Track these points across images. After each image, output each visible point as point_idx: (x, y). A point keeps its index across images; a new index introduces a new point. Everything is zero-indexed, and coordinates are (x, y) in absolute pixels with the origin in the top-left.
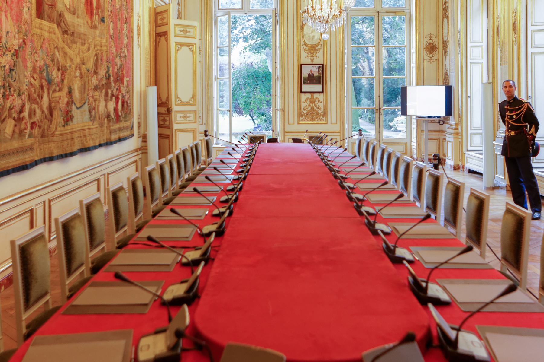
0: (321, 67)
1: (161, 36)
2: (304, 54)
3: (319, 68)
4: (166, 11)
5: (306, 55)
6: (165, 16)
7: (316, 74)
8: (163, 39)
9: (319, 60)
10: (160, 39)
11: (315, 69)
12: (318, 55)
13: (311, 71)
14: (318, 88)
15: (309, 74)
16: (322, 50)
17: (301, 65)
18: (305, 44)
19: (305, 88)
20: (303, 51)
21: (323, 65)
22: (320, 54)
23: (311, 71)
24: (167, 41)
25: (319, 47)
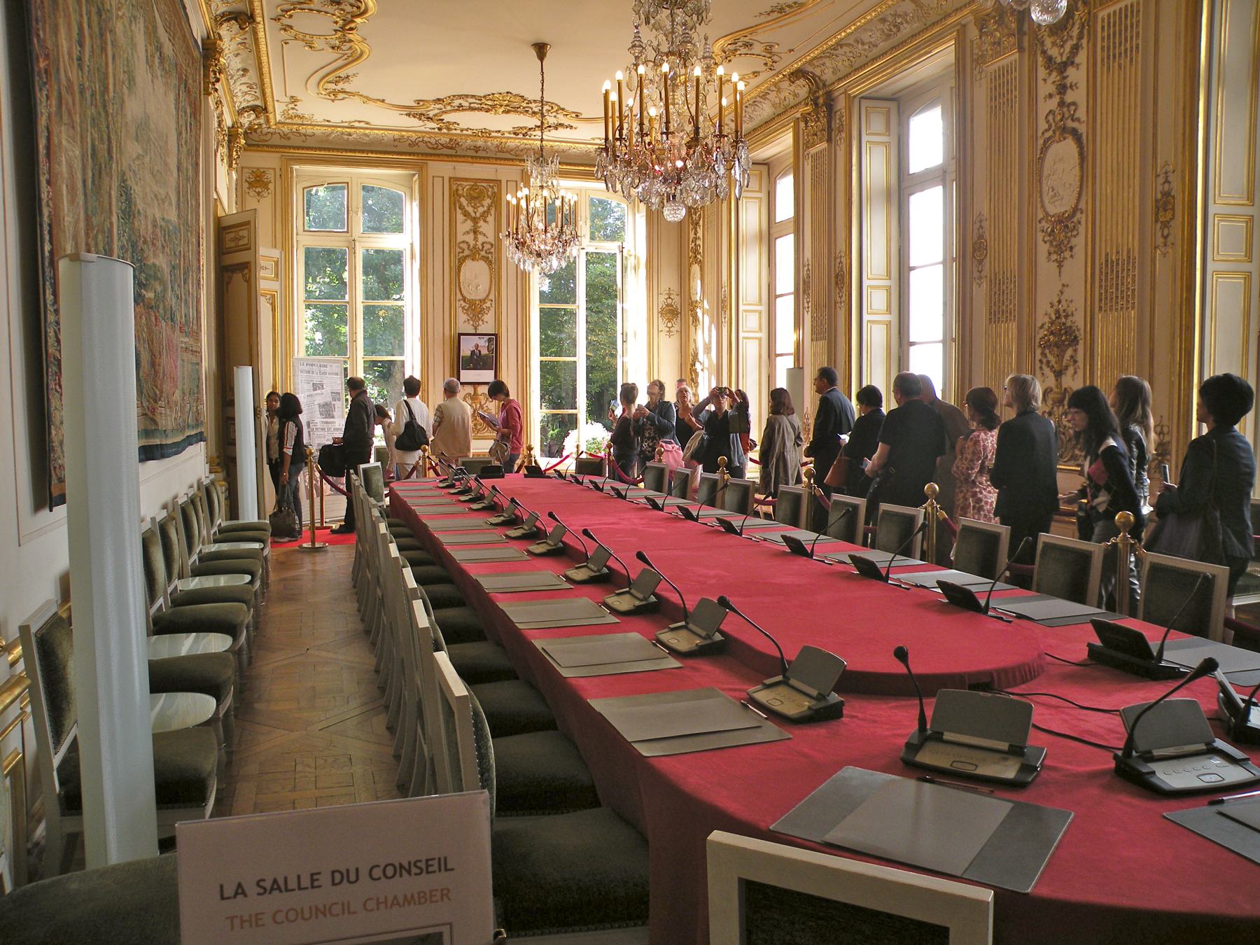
0: (494, 339)
1: (233, 272)
2: (462, 317)
3: (489, 340)
4: (248, 223)
5: (465, 317)
6: (244, 233)
7: (484, 352)
8: (238, 277)
9: (487, 326)
10: (230, 278)
11: (483, 343)
12: (486, 318)
13: (477, 346)
14: (488, 376)
15: (473, 352)
16: (492, 309)
17: (460, 335)
18: (464, 299)
19: (467, 375)
20: (460, 310)
21: (496, 335)
22: (489, 317)
23: (477, 346)
24: (248, 281)
25: (488, 304)
